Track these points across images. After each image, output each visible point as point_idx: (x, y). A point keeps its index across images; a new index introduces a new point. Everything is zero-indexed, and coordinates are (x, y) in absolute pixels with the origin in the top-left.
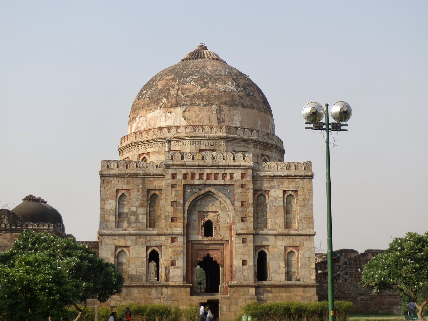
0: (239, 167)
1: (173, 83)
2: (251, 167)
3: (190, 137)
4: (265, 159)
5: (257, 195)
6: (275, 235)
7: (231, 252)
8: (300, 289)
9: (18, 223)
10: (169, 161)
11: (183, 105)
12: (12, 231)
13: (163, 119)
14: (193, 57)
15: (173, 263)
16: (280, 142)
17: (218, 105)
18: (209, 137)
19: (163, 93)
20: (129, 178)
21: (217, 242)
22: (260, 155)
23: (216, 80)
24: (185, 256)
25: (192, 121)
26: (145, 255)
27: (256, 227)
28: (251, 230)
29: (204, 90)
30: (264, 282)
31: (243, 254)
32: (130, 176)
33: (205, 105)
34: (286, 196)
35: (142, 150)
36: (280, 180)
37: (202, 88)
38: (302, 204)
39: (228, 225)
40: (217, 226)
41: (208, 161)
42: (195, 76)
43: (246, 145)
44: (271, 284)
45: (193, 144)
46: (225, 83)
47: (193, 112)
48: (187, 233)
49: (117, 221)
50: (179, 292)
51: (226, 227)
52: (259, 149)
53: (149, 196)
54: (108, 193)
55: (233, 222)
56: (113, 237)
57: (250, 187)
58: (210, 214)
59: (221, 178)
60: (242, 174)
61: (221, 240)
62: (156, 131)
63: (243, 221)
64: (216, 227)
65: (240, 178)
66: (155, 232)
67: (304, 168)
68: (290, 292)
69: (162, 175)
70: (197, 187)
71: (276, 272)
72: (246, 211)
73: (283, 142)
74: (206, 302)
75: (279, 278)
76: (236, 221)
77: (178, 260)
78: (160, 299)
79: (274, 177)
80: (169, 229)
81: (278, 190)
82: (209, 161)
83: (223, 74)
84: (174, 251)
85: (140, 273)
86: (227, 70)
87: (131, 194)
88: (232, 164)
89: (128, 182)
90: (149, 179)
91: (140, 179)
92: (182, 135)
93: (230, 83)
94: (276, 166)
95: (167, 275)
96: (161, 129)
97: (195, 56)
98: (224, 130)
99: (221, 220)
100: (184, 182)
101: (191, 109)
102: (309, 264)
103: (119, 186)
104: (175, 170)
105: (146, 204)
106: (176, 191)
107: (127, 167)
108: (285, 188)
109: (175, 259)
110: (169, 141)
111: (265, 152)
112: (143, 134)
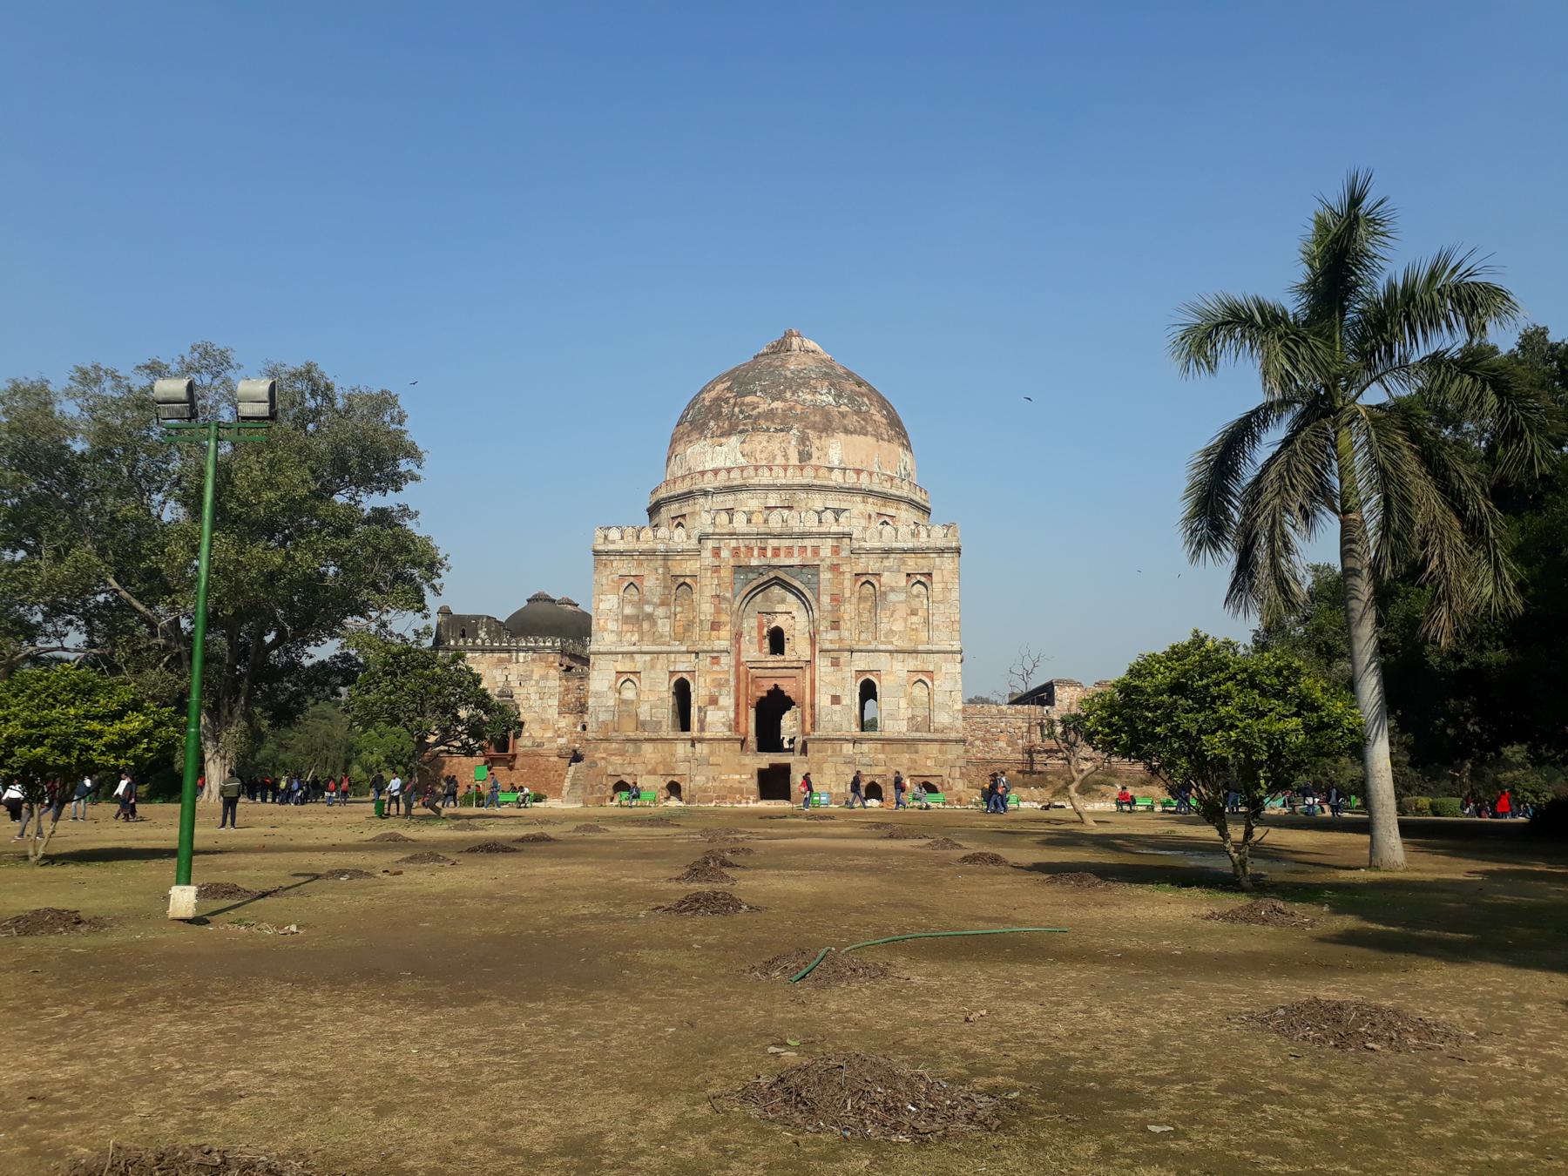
6: (891, 652)
7: (813, 682)
8: (935, 747)
12: (492, 651)
23: (800, 386)
29: (778, 405)
30: (872, 734)
32: (641, 553)
33: (777, 431)
66: (684, 648)
71: (892, 716)
79: (888, 552)
82: (775, 523)
96: (703, 473)
100: (732, 562)
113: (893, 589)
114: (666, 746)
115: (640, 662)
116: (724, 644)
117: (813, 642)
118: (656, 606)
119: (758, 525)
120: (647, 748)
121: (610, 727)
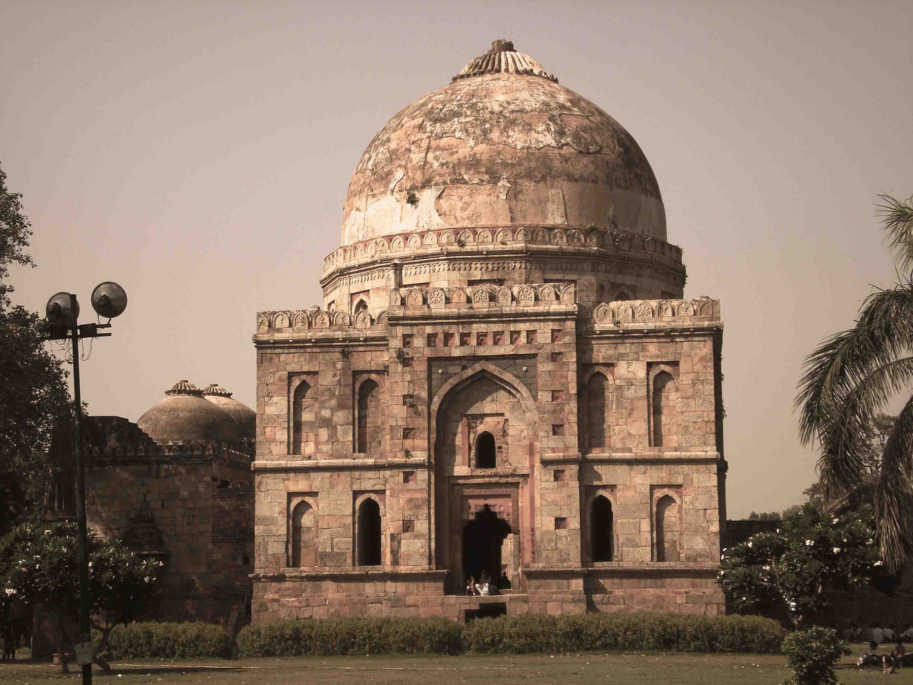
1: (419, 136)
2: (572, 313)
3: (449, 254)
5: (588, 376)
8: (686, 581)
10: (396, 308)
11: (436, 184)
15: (408, 526)
16: (667, 252)
18: (488, 253)
19: (399, 159)
20: (314, 350)
21: (504, 480)
22: (607, 286)
23: (512, 123)
24: (432, 511)
25: (455, 217)
27: (586, 445)
28: (574, 452)
29: (482, 148)
34: (653, 374)
35: (356, 284)
36: (640, 341)
37: (476, 144)
39: (527, 442)
40: (504, 446)
41: (479, 305)
42: (466, 116)
45: (454, 270)
46: (530, 130)
47: (456, 199)
48: (440, 461)
49: (292, 440)
50: (421, 588)
51: (523, 447)
52: (606, 271)
53: (357, 386)
54: (272, 380)
55: (535, 435)
56: (284, 475)
57: (572, 358)
58: (487, 419)
60: (553, 331)
61: (512, 475)
64: (500, 448)
66: (370, 461)
68: (662, 587)
69: (384, 339)
70: (457, 362)
72: (562, 410)
73: (678, 251)
74: (478, 608)
76: (541, 434)
78: (381, 603)
79: (625, 336)
80: (399, 455)
81: (634, 363)
82: (482, 306)
84: (410, 501)
85: (339, 549)
86: (543, 98)
87: (320, 382)
88: (530, 309)
90: (356, 349)
91: (337, 350)
92: (431, 251)
93: (541, 128)
94: (630, 311)
95: (395, 553)
96: (390, 238)
97: (480, 68)
98: (521, 237)
99: (511, 432)
100: (428, 352)
101: (454, 192)
102: (705, 524)
105: (351, 402)
106: (413, 373)
107: (310, 324)
108: (652, 357)
109: (412, 518)
110: (398, 268)
111: (619, 279)
112: (395, 244)
113: (630, 383)
115: (318, 481)
116: (420, 456)
117: (531, 451)
119: (458, 308)
120: (329, 585)
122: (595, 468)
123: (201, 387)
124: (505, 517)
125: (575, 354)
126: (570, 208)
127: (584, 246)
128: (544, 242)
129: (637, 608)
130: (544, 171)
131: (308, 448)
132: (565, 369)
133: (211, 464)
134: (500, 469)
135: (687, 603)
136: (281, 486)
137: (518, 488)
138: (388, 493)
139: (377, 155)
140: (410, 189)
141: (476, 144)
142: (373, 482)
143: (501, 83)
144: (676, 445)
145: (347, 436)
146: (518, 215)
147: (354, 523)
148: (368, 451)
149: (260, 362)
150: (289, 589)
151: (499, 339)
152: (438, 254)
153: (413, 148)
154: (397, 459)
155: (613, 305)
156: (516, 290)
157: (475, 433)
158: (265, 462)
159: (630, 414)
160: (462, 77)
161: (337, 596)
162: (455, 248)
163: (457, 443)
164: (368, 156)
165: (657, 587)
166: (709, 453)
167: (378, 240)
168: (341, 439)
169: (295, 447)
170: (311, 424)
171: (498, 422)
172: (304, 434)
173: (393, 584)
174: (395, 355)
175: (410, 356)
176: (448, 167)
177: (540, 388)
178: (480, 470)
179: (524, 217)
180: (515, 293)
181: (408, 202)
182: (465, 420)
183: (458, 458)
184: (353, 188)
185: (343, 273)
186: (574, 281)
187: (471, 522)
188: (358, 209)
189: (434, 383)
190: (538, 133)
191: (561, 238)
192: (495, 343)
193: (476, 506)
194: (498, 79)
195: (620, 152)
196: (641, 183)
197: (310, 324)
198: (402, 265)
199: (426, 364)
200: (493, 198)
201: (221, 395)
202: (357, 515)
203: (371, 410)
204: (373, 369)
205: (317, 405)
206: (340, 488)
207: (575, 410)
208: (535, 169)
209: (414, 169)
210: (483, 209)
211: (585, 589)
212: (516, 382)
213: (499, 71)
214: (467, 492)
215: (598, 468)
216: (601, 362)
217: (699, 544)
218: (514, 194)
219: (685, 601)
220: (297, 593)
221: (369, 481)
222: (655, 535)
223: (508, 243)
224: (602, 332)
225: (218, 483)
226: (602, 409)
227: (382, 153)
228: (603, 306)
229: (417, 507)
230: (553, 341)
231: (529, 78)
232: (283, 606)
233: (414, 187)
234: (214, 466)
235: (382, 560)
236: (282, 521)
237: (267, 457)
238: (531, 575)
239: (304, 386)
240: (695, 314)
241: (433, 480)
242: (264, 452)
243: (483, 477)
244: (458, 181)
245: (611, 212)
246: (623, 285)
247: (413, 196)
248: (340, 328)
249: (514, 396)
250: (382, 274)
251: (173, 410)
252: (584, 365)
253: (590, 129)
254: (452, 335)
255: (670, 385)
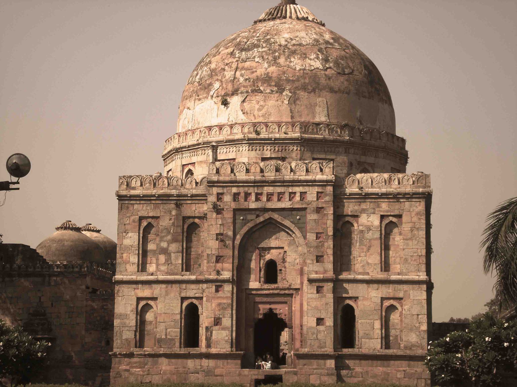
0: (312, 183)
1: (230, 60)
2: (331, 181)
3: (249, 139)
4: (365, 168)
5: (341, 223)
6: (368, 282)
7: (301, 305)
8: (404, 363)
9: (37, 264)
10: (213, 175)
11: (242, 93)
13: (215, 115)
14: (270, 16)
15: (217, 322)
17: (293, 91)
18: (276, 139)
19: (217, 75)
20: (157, 202)
21: (283, 292)
23: (294, 53)
24: (234, 312)
25: (254, 115)
26: (178, 311)
27: (339, 270)
28: (330, 274)
29: (273, 69)
31: (318, 309)
35: (186, 158)
36: (376, 200)
37: (269, 66)
38: (409, 236)
39: (299, 267)
40: (283, 269)
42: (263, 47)
43: (333, 149)
44: (360, 353)
45: (252, 150)
46: (306, 57)
47: (255, 103)
48: (240, 279)
49: (140, 262)
50: (225, 364)
51: (295, 270)
53: (186, 227)
55: (304, 262)
56: (134, 286)
57: (331, 211)
58: (273, 251)
59: (288, 199)
60: (318, 193)
61: (289, 289)
62: (204, 132)
63: (317, 262)
64: (281, 270)
65: (316, 200)
66: (193, 277)
67: (412, 183)
68: (388, 366)
69: (204, 195)
70: (253, 212)
71: (368, 336)
72: (323, 246)
73: (403, 141)
74: (264, 378)
75: (372, 345)
76: (308, 261)
77: (224, 317)
78: (198, 373)
79: (366, 197)
80: (212, 274)
81: (372, 215)
82: (271, 175)
83: (304, 43)
84: (219, 304)
85: (171, 336)
86: (315, 36)
87: (161, 224)
88: (302, 178)
89: (156, 206)
90: (185, 202)
91: (173, 202)
92: (237, 137)
93: (313, 56)
95: (208, 339)
96: (210, 128)
97: (273, 15)
98: (297, 129)
99: (288, 259)
100: (233, 205)
103: (143, 212)
104: (221, 188)
105: (181, 237)
106: (223, 219)
107: (155, 185)
108: (384, 211)
109: (221, 316)
110: (214, 148)
111: (363, 159)
112: (213, 132)
113: (369, 229)
114: (180, 361)
115: (157, 290)
117: (301, 272)
118: (169, 243)
120: (163, 361)
121: (133, 343)
122: (344, 285)
123: (79, 225)
124: (283, 317)
125: (332, 208)
126: (331, 110)
127: (340, 136)
128: (312, 133)
129: (370, 380)
130: (314, 86)
131: (152, 268)
132: (326, 218)
133: (86, 277)
134: (280, 284)
135: (405, 378)
136: (133, 293)
137: (292, 297)
138: (204, 299)
139: (202, 73)
140: (224, 96)
141: (269, 66)
142: (195, 291)
143: (287, 26)
144: (399, 271)
145: (178, 261)
146: (296, 115)
147: (181, 319)
148: (192, 270)
149: (121, 209)
150: (136, 363)
151: (282, 197)
152: (242, 140)
153: (226, 68)
154: (211, 277)
155: (359, 176)
156: (293, 165)
157: (264, 260)
158: (122, 277)
159: (369, 250)
160: (260, 21)
161: (168, 368)
162: (253, 136)
163: (252, 266)
164: (196, 72)
165: (384, 366)
166: (421, 277)
167: (202, 129)
168: (173, 262)
169: (142, 267)
170: (154, 252)
171: (280, 253)
172: (149, 259)
173: (207, 361)
174: (211, 207)
175: (221, 208)
176: (249, 81)
177: (308, 230)
178: (267, 285)
179: (300, 116)
180: (293, 167)
181: (222, 104)
182: (257, 251)
183: (253, 277)
184: (186, 93)
185: (178, 151)
186: (333, 160)
187: (260, 320)
188: (188, 108)
189: (238, 226)
190: (311, 59)
191: (325, 130)
192: (279, 200)
193: (264, 309)
194: (285, 23)
195: (365, 74)
196: (379, 95)
197: (155, 185)
198: (217, 146)
199: (232, 213)
200: (280, 103)
201: (93, 231)
202: (183, 313)
203: (194, 243)
204: (196, 215)
205: (158, 239)
206: (172, 295)
207: (332, 246)
208: (308, 84)
209: (227, 82)
210: (273, 110)
211: (336, 367)
212: (292, 227)
213: (285, 17)
214: (258, 299)
215: (346, 285)
216: (350, 214)
217: (413, 338)
218: (294, 100)
219: (403, 376)
220: (142, 366)
221: (192, 291)
222: (383, 331)
223: (289, 133)
224: (351, 194)
225: (90, 290)
226: (350, 246)
227: (205, 71)
228: (352, 177)
229: (224, 309)
230: (318, 199)
231: (305, 22)
232: (132, 374)
233: (226, 95)
234: (88, 279)
235: (200, 344)
236: (133, 317)
237: (124, 273)
238: (300, 356)
239: (149, 226)
240: (413, 184)
241: (235, 291)
242: (122, 270)
243: (269, 289)
244: (256, 91)
245: (358, 114)
246: (365, 162)
247: (226, 100)
248: (175, 188)
249: (291, 236)
250: (203, 152)
251: (60, 241)
252: (338, 216)
253: (346, 58)
254: (250, 194)
255: (396, 230)
